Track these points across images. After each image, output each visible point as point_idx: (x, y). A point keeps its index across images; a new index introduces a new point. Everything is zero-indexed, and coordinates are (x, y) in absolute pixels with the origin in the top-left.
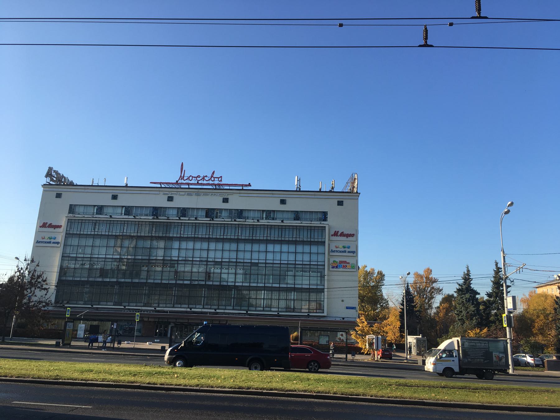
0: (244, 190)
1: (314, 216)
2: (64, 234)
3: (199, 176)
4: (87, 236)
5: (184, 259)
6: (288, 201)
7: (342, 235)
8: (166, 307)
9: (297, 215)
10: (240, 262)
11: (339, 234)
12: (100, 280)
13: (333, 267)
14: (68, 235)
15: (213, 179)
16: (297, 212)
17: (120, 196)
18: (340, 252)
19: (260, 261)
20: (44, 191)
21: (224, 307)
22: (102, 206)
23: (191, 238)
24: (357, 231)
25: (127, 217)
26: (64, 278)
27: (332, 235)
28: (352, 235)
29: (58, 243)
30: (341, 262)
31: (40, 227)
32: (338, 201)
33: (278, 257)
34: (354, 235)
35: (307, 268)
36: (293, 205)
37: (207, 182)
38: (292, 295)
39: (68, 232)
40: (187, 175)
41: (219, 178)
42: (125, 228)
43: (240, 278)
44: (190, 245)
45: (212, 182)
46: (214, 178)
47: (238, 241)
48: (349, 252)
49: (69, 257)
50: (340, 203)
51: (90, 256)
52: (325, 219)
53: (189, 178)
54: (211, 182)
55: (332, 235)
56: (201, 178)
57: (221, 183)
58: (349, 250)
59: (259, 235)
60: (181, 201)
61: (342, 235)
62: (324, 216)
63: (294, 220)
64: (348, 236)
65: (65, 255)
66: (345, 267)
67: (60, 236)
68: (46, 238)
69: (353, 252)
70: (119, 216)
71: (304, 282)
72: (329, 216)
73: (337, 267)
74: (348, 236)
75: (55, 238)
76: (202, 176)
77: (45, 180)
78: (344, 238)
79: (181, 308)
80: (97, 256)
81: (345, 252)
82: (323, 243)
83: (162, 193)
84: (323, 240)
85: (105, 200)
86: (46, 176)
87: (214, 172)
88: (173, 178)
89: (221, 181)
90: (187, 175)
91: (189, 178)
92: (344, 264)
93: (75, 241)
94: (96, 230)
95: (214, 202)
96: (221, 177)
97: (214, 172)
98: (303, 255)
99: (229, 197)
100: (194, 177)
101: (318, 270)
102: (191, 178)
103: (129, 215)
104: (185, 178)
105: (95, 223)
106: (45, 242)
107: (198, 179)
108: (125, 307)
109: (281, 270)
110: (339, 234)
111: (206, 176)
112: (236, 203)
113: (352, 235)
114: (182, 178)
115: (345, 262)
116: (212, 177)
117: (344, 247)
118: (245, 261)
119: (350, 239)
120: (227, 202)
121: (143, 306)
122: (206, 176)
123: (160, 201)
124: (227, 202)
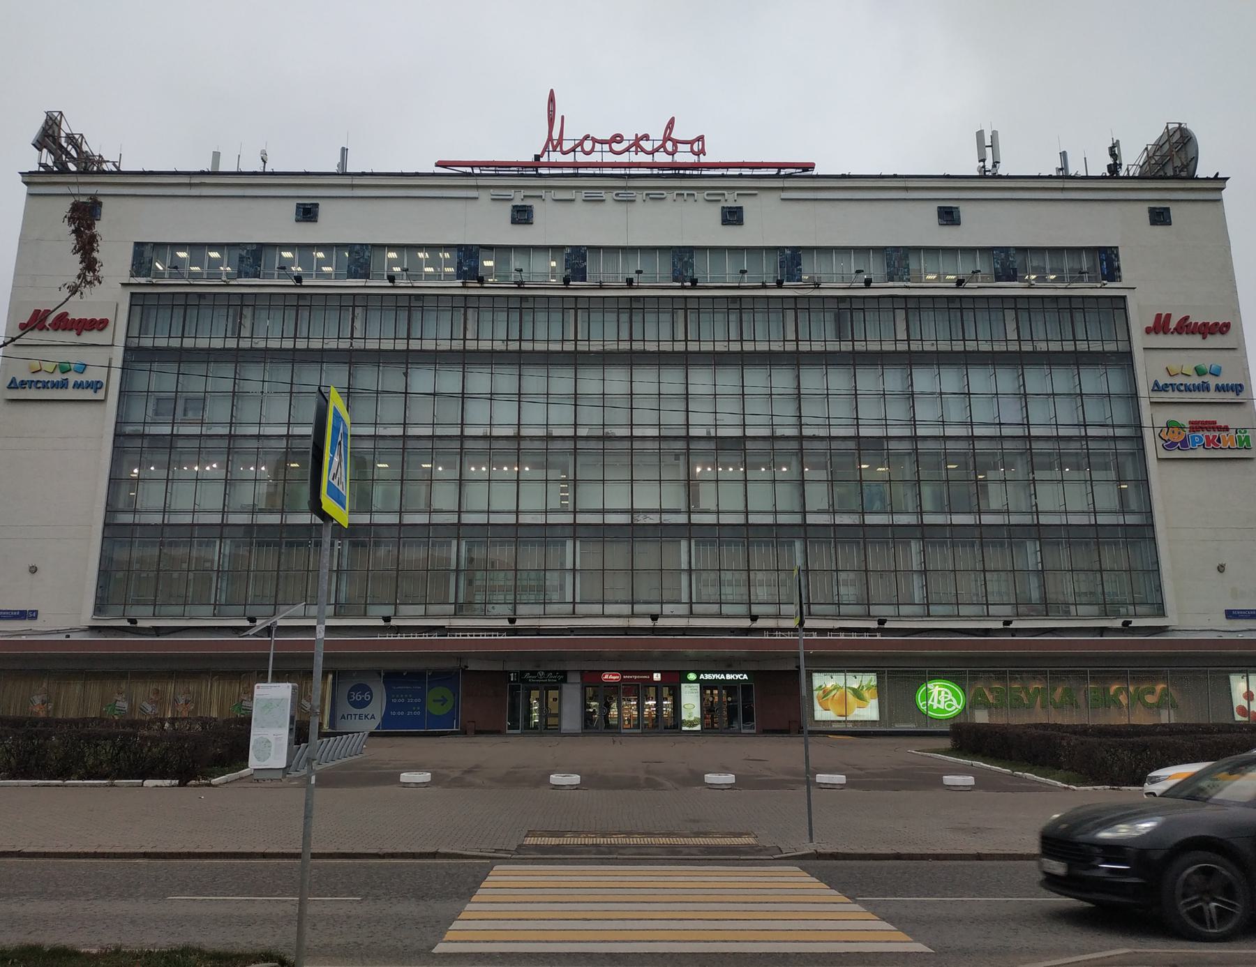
0: (795, 179)
1: (1067, 263)
2: (118, 355)
3: (617, 138)
4: (210, 356)
5: (599, 433)
6: (966, 211)
7: (1185, 327)
8: (545, 616)
9: (1007, 262)
10: (814, 438)
11: (1173, 325)
12: (275, 519)
13: (1170, 446)
14: (135, 356)
15: (669, 145)
16: (1005, 250)
17: (325, 209)
18: (1188, 389)
19: (893, 432)
20: (30, 195)
21: (714, 608)
22: (262, 246)
23: (618, 353)
24: (1236, 312)
25: (361, 282)
26: (127, 518)
27: (1148, 331)
28: (1223, 329)
29: (95, 386)
30: (1196, 426)
31: (24, 327)
32: (1152, 210)
33: (955, 412)
34: (1227, 325)
35: (1075, 453)
36: (986, 226)
37: (648, 159)
38: (1031, 555)
39: (134, 343)
40: (573, 133)
41: (691, 143)
42: (358, 324)
43: (817, 496)
44: (616, 381)
45: (668, 159)
46: (676, 142)
47: (796, 360)
48: (1219, 388)
49: (143, 436)
50: (1160, 217)
51: (225, 431)
52: (1112, 273)
53: (581, 144)
54: (661, 158)
55: (1148, 331)
56: (625, 145)
57: (703, 159)
58: (1221, 381)
59: (876, 336)
60: (562, 224)
61: (1185, 327)
62: (1106, 261)
63: (998, 279)
64: (1206, 330)
65: (129, 429)
66: (1214, 443)
67: (104, 358)
68: (49, 367)
69: (1238, 389)
70: (328, 277)
71: (1064, 500)
72: (1124, 262)
73: (1184, 444)
74: (1206, 330)
75: (83, 368)
76: (629, 136)
77: (33, 159)
78: (1195, 341)
79: (603, 616)
80: (254, 430)
81: (1205, 387)
82: (1125, 359)
83: (485, 196)
84: (1122, 347)
85: (272, 223)
86: (39, 144)
87: (672, 122)
88: (523, 145)
89: (702, 152)
90: (573, 133)
91: (581, 144)
92: (1211, 434)
93: (164, 380)
94: (245, 332)
95: (694, 224)
96: (701, 138)
97: (672, 122)
98: (1054, 404)
99: (747, 204)
100: (602, 142)
101: (1124, 456)
102: (588, 145)
103: (367, 276)
104: (567, 146)
105: (239, 305)
106: (45, 385)
107: (616, 147)
108: (882, 622)
109: (974, 459)
110: (1173, 325)
111: (646, 137)
112: (770, 223)
113: (1223, 329)
114: (554, 143)
115: (1210, 426)
116: (667, 138)
117: (1199, 372)
118: (835, 432)
119: (1214, 341)
120: (740, 222)
121: (455, 615)
122: (646, 137)
123: (485, 223)
124: (740, 222)
